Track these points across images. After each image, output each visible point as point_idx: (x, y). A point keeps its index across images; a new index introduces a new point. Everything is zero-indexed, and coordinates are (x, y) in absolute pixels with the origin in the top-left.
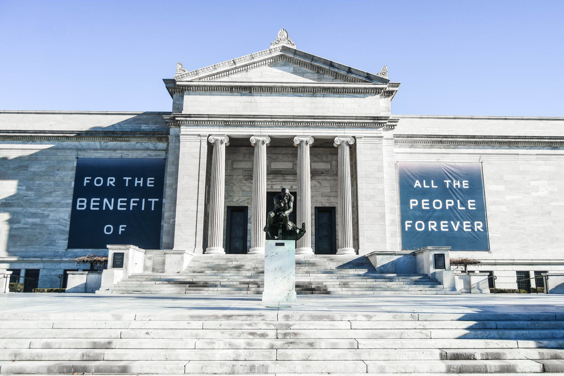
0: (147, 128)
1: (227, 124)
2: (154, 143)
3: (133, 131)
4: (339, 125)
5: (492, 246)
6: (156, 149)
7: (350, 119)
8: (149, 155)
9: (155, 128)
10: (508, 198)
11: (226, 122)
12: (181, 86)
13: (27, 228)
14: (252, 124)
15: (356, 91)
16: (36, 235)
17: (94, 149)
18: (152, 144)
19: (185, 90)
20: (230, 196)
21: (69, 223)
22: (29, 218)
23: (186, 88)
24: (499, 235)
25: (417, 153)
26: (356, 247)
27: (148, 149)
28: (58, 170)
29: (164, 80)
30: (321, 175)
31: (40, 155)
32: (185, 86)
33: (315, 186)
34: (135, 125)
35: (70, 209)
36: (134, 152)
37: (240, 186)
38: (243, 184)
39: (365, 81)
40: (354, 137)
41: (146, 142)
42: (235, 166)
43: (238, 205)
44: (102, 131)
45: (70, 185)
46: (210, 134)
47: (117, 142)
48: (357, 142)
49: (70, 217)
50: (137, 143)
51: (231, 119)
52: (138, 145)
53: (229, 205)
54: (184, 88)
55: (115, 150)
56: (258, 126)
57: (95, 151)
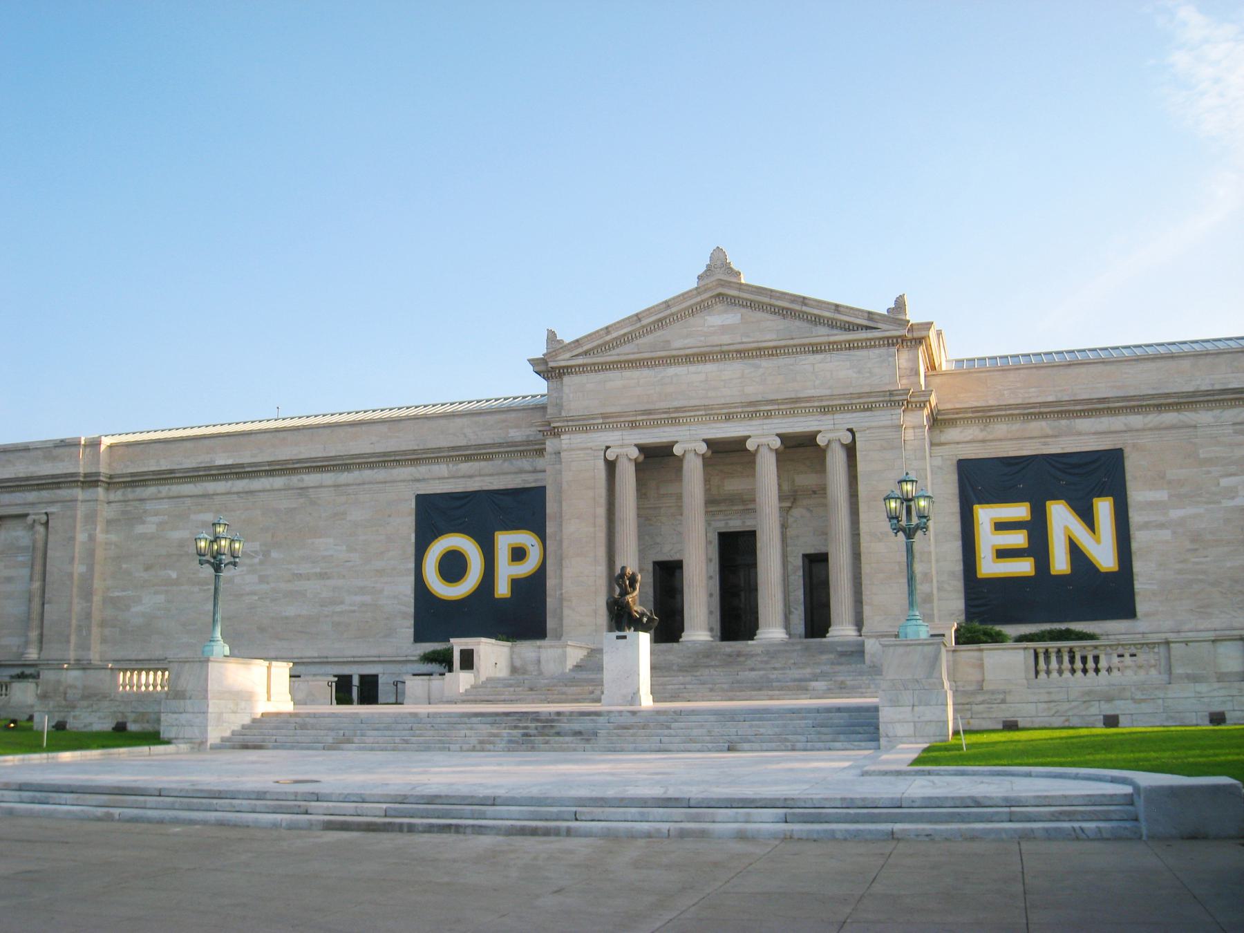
0: (517, 434)
1: (633, 425)
2: (531, 460)
3: (496, 442)
4: (823, 410)
5: (1141, 607)
6: (535, 469)
7: (840, 399)
8: (524, 481)
9: (528, 433)
10: (1175, 514)
11: (632, 422)
12: (556, 368)
13: (354, 611)
14: (674, 422)
15: (851, 345)
16: (367, 622)
17: (439, 479)
18: (528, 461)
19: (564, 374)
20: (658, 544)
21: (413, 601)
22: (356, 595)
23: (565, 371)
24: (1155, 587)
25: (996, 440)
26: (859, 624)
27: (521, 471)
28: (390, 516)
29: (528, 360)
30: (813, 496)
31: (362, 493)
32: (563, 367)
33: (802, 517)
34: (500, 431)
35: (412, 578)
36: (501, 477)
37: (673, 524)
38: (678, 522)
39: (867, 328)
40: (851, 430)
41: (517, 459)
42: (662, 492)
43: (671, 559)
44: (448, 448)
45: (410, 540)
46: (608, 444)
47: (472, 463)
48: (857, 439)
49: (413, 592)
50: (505, 461)
51: (639, 418)
52: (506, 464)
53: (655, 560)
54: (561, 371)
55: (471, 477)
56: (684, 424)
57: (441, 481)
